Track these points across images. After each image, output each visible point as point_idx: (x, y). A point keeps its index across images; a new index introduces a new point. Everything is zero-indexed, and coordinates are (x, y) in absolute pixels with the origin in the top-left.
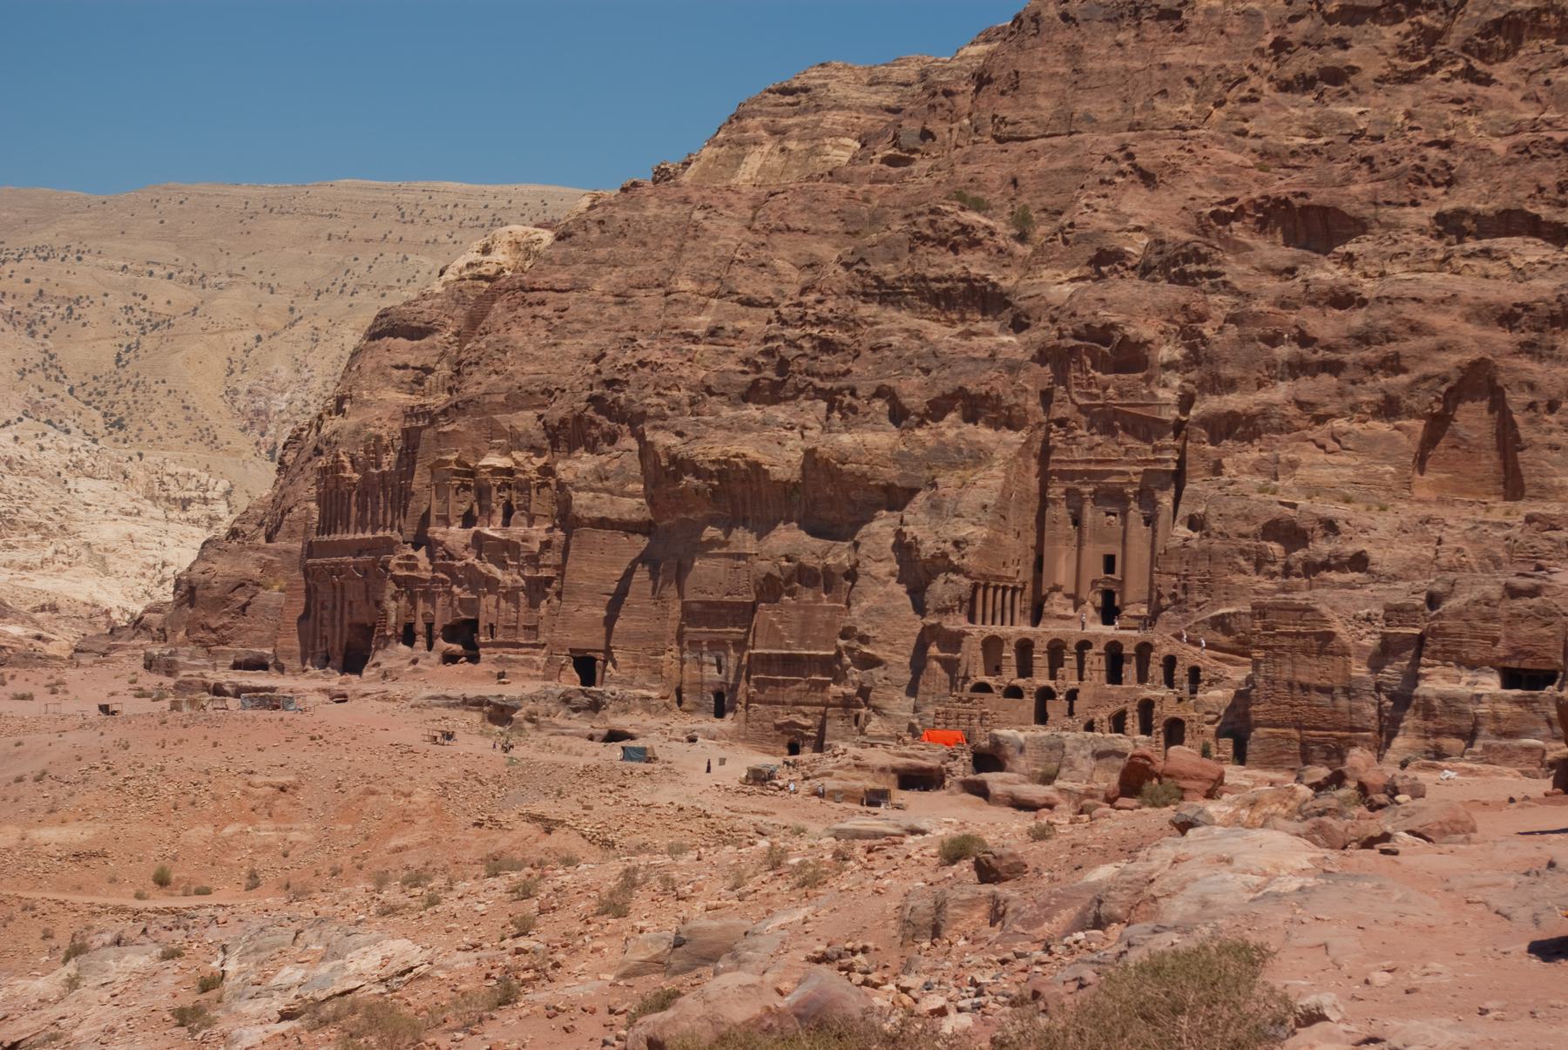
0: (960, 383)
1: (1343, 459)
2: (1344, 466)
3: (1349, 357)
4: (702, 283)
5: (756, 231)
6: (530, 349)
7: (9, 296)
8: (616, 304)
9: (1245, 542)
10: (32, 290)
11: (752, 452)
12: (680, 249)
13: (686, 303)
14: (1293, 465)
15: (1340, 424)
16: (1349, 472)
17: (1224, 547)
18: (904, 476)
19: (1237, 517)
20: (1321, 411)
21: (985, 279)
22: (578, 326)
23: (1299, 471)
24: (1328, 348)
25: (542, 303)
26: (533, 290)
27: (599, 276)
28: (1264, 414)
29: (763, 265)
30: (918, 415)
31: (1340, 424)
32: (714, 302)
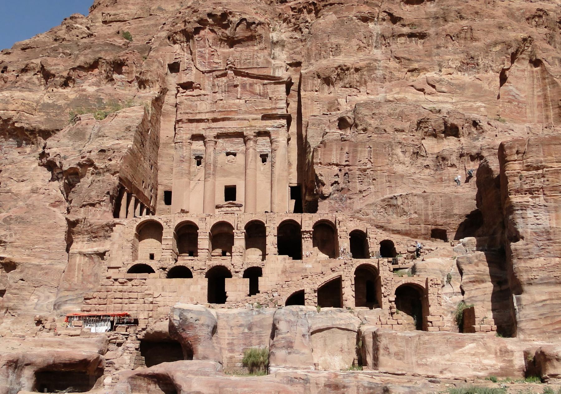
3: (432, 31)
9: (400, 136)
17: (382, 140)
19: (390, 115)
20: (416, 65)
24: (412, 25)
28: (371, 68)
30: (62, 77)
31: (432, 75)
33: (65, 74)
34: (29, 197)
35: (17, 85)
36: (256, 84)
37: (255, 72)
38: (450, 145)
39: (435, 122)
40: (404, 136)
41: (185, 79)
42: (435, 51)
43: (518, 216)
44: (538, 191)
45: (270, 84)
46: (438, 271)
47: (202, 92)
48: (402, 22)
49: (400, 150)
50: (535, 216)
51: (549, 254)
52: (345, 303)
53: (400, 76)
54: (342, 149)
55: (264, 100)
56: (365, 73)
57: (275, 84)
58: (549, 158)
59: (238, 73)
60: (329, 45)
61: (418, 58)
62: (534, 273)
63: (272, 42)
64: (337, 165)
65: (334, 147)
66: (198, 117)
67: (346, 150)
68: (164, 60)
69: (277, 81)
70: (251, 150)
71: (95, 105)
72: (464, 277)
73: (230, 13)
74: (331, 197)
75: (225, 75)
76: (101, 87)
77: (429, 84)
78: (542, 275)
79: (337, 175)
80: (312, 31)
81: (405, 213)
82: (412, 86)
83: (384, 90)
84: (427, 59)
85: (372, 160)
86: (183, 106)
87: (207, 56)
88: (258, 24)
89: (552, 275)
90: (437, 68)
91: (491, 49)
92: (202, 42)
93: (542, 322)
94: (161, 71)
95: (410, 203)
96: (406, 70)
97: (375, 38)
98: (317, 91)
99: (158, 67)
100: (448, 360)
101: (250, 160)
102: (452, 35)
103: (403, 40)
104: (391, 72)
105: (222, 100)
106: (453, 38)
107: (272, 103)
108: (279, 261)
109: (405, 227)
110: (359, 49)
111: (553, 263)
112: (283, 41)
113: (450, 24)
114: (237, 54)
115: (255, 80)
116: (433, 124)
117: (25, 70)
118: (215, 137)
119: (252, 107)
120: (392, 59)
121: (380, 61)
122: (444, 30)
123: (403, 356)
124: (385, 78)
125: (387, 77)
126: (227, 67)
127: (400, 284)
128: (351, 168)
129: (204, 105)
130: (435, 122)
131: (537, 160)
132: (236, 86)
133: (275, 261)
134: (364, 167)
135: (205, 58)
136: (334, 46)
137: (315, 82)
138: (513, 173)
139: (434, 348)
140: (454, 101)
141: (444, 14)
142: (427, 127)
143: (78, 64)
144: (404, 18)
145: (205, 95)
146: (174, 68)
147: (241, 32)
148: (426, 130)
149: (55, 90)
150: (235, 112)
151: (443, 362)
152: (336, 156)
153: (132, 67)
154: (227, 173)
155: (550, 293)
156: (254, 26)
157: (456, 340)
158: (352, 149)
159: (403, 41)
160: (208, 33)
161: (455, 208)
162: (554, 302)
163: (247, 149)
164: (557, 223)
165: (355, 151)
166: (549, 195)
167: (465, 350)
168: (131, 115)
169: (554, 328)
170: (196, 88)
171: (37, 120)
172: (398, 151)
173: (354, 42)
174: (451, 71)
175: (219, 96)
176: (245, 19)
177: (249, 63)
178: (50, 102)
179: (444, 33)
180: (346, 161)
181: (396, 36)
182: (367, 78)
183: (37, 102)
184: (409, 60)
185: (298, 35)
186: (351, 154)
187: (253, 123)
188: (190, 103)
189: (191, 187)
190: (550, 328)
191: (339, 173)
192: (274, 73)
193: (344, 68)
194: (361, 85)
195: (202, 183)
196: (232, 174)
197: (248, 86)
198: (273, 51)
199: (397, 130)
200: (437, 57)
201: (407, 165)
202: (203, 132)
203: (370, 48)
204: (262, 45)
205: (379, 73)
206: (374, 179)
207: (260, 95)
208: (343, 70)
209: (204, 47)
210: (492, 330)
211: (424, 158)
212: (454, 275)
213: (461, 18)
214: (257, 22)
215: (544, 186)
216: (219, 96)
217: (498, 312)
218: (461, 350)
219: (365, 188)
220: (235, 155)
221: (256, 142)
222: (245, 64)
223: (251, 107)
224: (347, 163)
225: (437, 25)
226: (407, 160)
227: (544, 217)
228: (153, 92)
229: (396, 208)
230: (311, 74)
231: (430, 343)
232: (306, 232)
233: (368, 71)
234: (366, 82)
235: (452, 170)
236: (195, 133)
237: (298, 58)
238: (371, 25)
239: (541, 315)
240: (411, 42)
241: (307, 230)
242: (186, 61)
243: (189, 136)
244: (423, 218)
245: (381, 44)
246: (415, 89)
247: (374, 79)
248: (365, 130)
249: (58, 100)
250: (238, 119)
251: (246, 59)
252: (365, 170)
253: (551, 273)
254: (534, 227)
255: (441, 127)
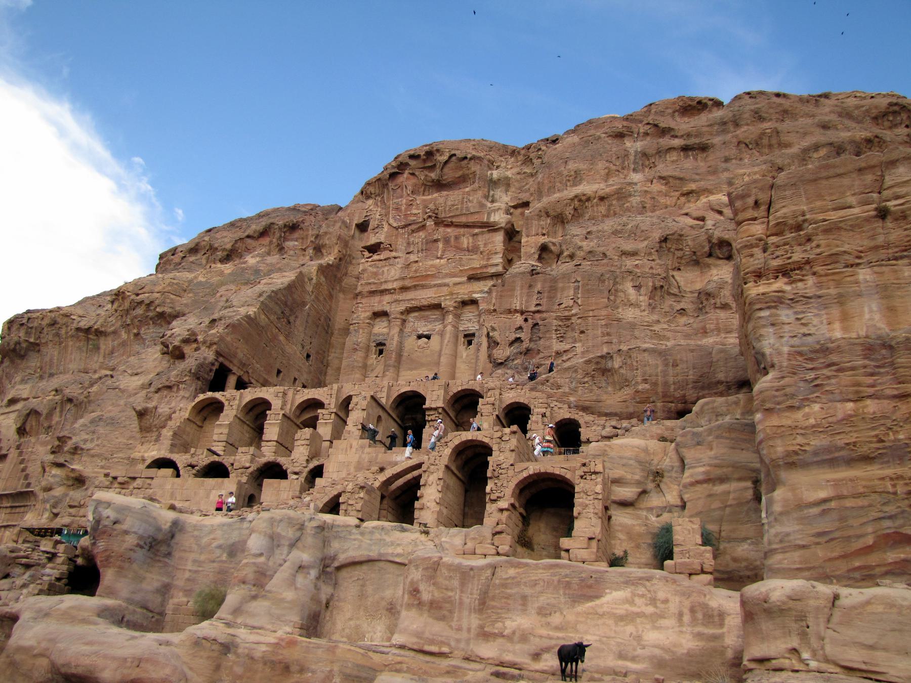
3: (717, 140)
9: (629, 263)
17: (599, 270)
20: (693, 186)
28: (621, 195)
33: (229, 247)
36: (464, 235)
37: (463, 220)
39: (694, 240)
40: (637, 262)
41: (373, 240)
42: (724, 165)
43: (763, 322)
44: (800, 268)
45: (482, 233)
46: (631, 462)
47: (394, 254)
48: (672, 133)
49: (631, 284)
50: (798, 319)
51: (831, 396)
52: (417, 514)
53: (668, 203)
54: (530, 286)
56: (614, 202)
57: (489, 231)
58: (818, 203)
59: (439, 222)
60: (565, 173)
62: (800, 440)
63: (491, 180)
64: (522, 313)
65: (519, 283)
66: (384, 287)
67: (539, 287)
69: (491, 228)
72: (687, 473)
73: (438, 151)
74: (510, 364)
75: (423, 227)
77: (712, 209)
78: (817, 442)
79: (520, 328)
80: (545, 159)
81: (626, 383)
82: (687, 214)
85: (579, 301)
86: (366, 275)
88: (471, 159)
89: (840, 441)
91: (810, 155)
92: (399, 190)
93: (820, 553)
94: (344, 232)
95: (635, 364)
96: (677, 194)
97: (632, 158)
98: (544, 235)
100: (558, 628)
101: (446, 341)
102: (747, 141)
103: (673, 156)
104: (654, 198)
105: (417, 262)
106: (750, 146)
107: (483, 259)
108: (354, 450)
109: (627, 407)
111: (840, 415)
113: (745, 128)
114: (441, 200)
115: (462, 230)
116: (690, 243)
118: (402, 313)
120: (655, 181)
121: (636, 184)
122: (737, 136)
123: (451, 612)
124: (644, 207)
125: (648, 206)
126: (425, 217)
127: (525, 474)
128: (544, 315)
129: (393, 271)
130: (695, 240)
131: (794, 211)
132: (436, 241)
133: (346, 450)
134: (567, 314)
135: (401, 211)
136: (573, 173)
138: (748, 241)
139: (524, 598)
142: (682, 250)
145: (395, 258)
146: (363, 227)
147: (450, 174)
148: (679, 254)
149: (213, 266)
150: (433, 276)
151: (544, 632)
152: (521, 297)
153: (308, 230)
155: (837, 483)
156: (466, 161)
157: (582, 580)
158: (547, 285)
159: (675, 158)
161: (718, 370)
162: (849, 503)
164: (845, 329)
166: (822, 273)
167: (602, 606)
169: (850, 567)
170: (385, 249)
173: (601, 165)
175: (413, 257)
176: (454, 155)
177: (457, 209)
179: (735, 140)
180: (537, 305)
181: (662, 152)
182: (618, 210)
184: (681, 179)
185: (528, 170)
186: (546, 295)
187: (456, 289)
188: (375, 270)
190: (842, 567)
191: (524, 325)
193: (584, 198)
197: (452, 239)
198: (492, 193)
199: (624, 253)
200: (725, 173)
201: (643, 308)
202: (387, 308)
203: (625, 172)
204: (476, 185)
205: (635, 200)
206: (582, 332)
207: (468, 251)
208: (583, 200)
209: (402, 197)
210: (703, 572)
211: (678, 299)
212: (669, 472)
213: (761, 119)
214: (469, 156)
215: (811, 257)
216: (413, 257)
217: (752, 543)
218: (590, 604)
219: (568, 347)
223: (454, 268)
224: (539, 308)
225: (724, 132)
226: (643, 299)
227: (815, 321)
229: (612, 374)
230: (537, 212)
231: (518, 584)
232: (431, 409)
233: (618, 199)
235: (722, 314)
236: (376, 309)
237: (525, 197)
239: (819, 535)
241: (433, 406)
243: (369, 314)
244: (660, 390)
245: (643, 165)
246: (691, 218)
247: (628, 209)
248: (572, 256)
249: (212, 277)
250: (435, 285)
251: (453, 205)
252: (568, 318)
253: (838, 437)
254: (795, 341)
255: (703, 247)
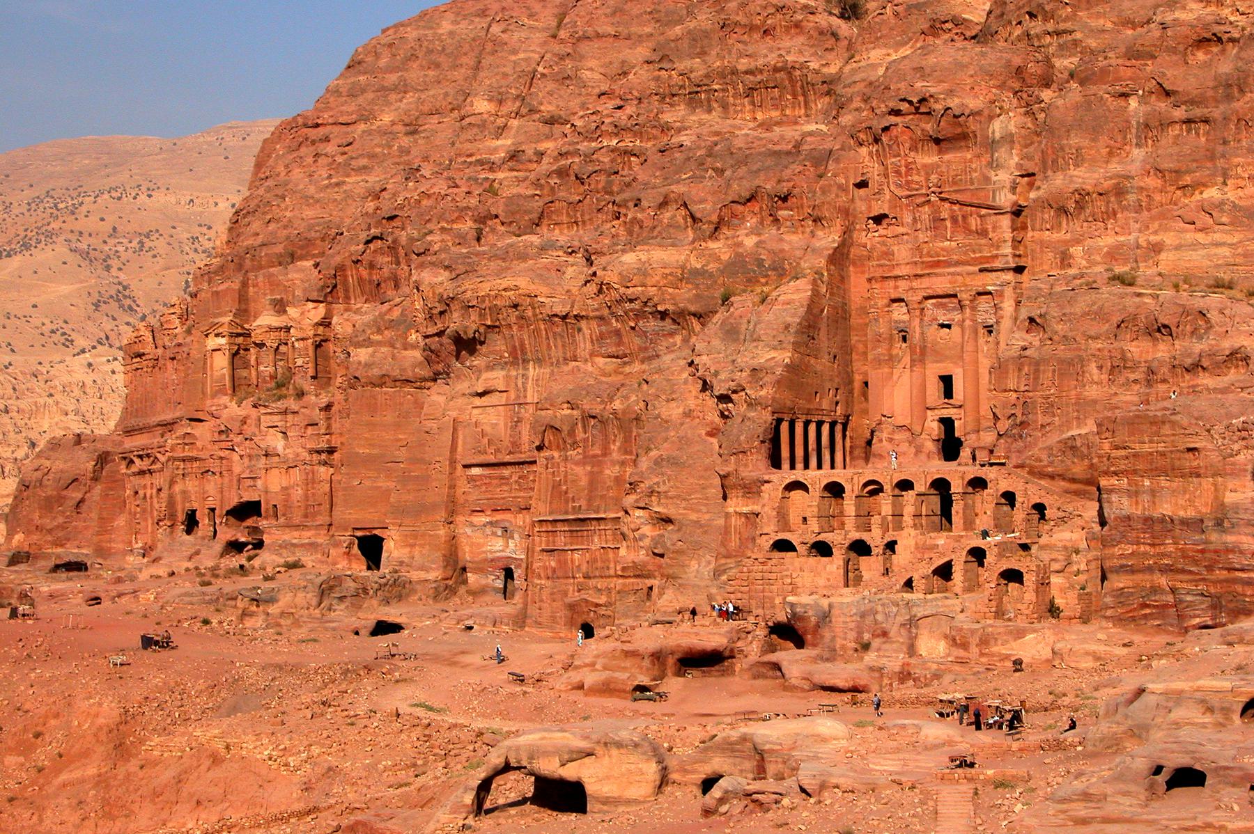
0: (757, 182)
1: (1217, 237)
2: (1217, 245)
3: (1216, 113)
4: (500, 102)
5: (562, 41)
6: (312, 190)
7: (86, 234)
8: (407, 134)
9: (1095, 345)
10: (106, 227)
11: (523, 283)
12: (477, 67)
13: (482, 126)
14: (1157, 248)
15: (1212, 193)
16: (1225, 251)
17: (1069, 355)
18: (698, 297)
20: (1188, 179)
21: (804, 66)
22: (364, 162)
23: (1163, 256)
25: (327, 139)
26: (317, 126)
27: (389, 104)
28: (1120, 192)
29: (569, 77)
30: (710, 222)
31: (1212, 193)
32: (515, 123)
34: (682, 424)
35: (655, 234)
38: (1162, 351)
40: (1100, 346)
47: (901, 230)
55: (983, 241)
60: (1067, 150)
61: (1195, 165)
65: (1011, 367)
66: (897, 272)
68: (847, 179)
69: (999, 211)
70: (968, 323)
71: (754, 272)
73: (931, 96)
76: (763, 238)
83: (1137, 226)
84: (1209, 165)
87: (903, 170)
90: (1220, 180)
97: (1134, 131)
99: (837, 196)
103: (1174, 131)
110: (1111, 154)
112: (1012, 135)
117: (664, 204)
119: (965, 253)
128: (1031, 394)
137: (1046, 216)
140: (1235, 240)
141: (1239, 79)
143: (730, 199)
144: (1180, 89)
147: (946, 129)
154: (940, 357)
160: (903, 132)
163: (964, 321)
165: (1037, 371)
168: (795, 297)
171: (684, 297)
172: (1093, 368)
173: (1104, 140)
174: (1242, 183)
178: (699, 266)
183: (683, 268)
184: (1176, 172)
188: (884, 249)
189: (895, 377)
192: (994, 197)
194: (1109, 218)
195: (908, 371)
196: (947, 357)
197: (960, 218)
203: (1127, 148)
204: (977, 150)
205: (1132, 198)
208: (1082, 197)
216: (922, 236)
220: (949, 326)
221: (973, 309)
222: (955, 183)
228: (828, 239)
234: (1115, 214)
236: (893, 297)
238: (1133, 103)
240: (1189, 131)
242: (877, 178)
243: (886, 301)
